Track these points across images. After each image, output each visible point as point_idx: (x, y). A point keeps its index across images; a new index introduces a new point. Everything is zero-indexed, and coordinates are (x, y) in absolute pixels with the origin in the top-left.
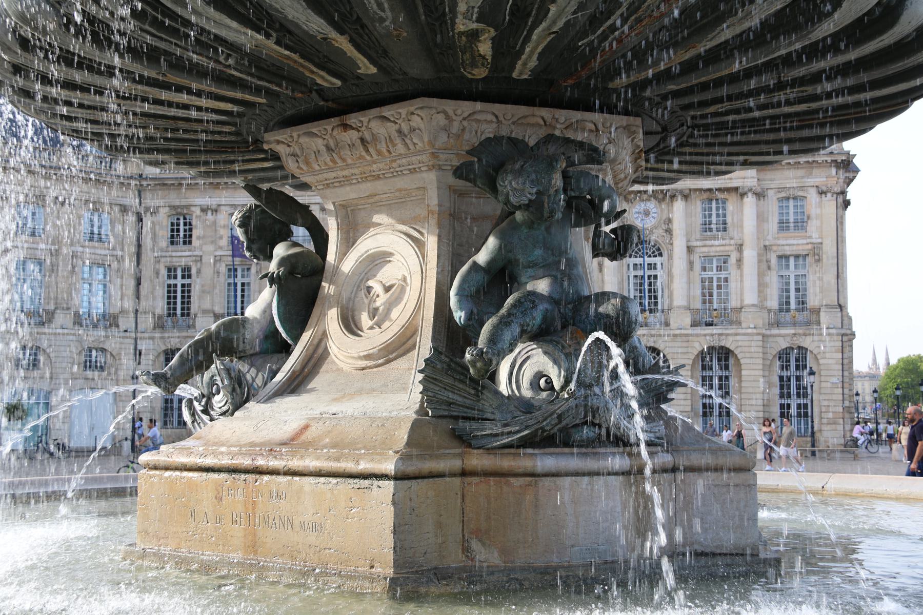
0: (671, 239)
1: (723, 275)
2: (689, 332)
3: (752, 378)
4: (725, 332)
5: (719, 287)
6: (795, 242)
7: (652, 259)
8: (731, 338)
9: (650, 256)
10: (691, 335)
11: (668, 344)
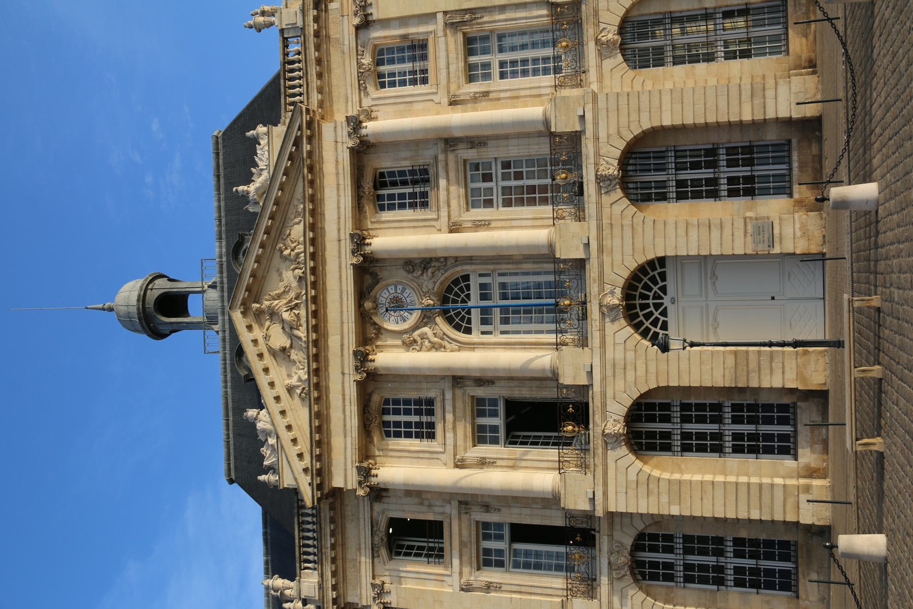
0: (437, 259)
1: (497, 171)
2: (593, 223)
3: (678, 107)
4: (592, 160)
5: (519, 176)
6: (442, 55)
7: (472, 292)
8: (605, 149)
9: (468, 296)
10: (599, 219)
11: (617, 257)
